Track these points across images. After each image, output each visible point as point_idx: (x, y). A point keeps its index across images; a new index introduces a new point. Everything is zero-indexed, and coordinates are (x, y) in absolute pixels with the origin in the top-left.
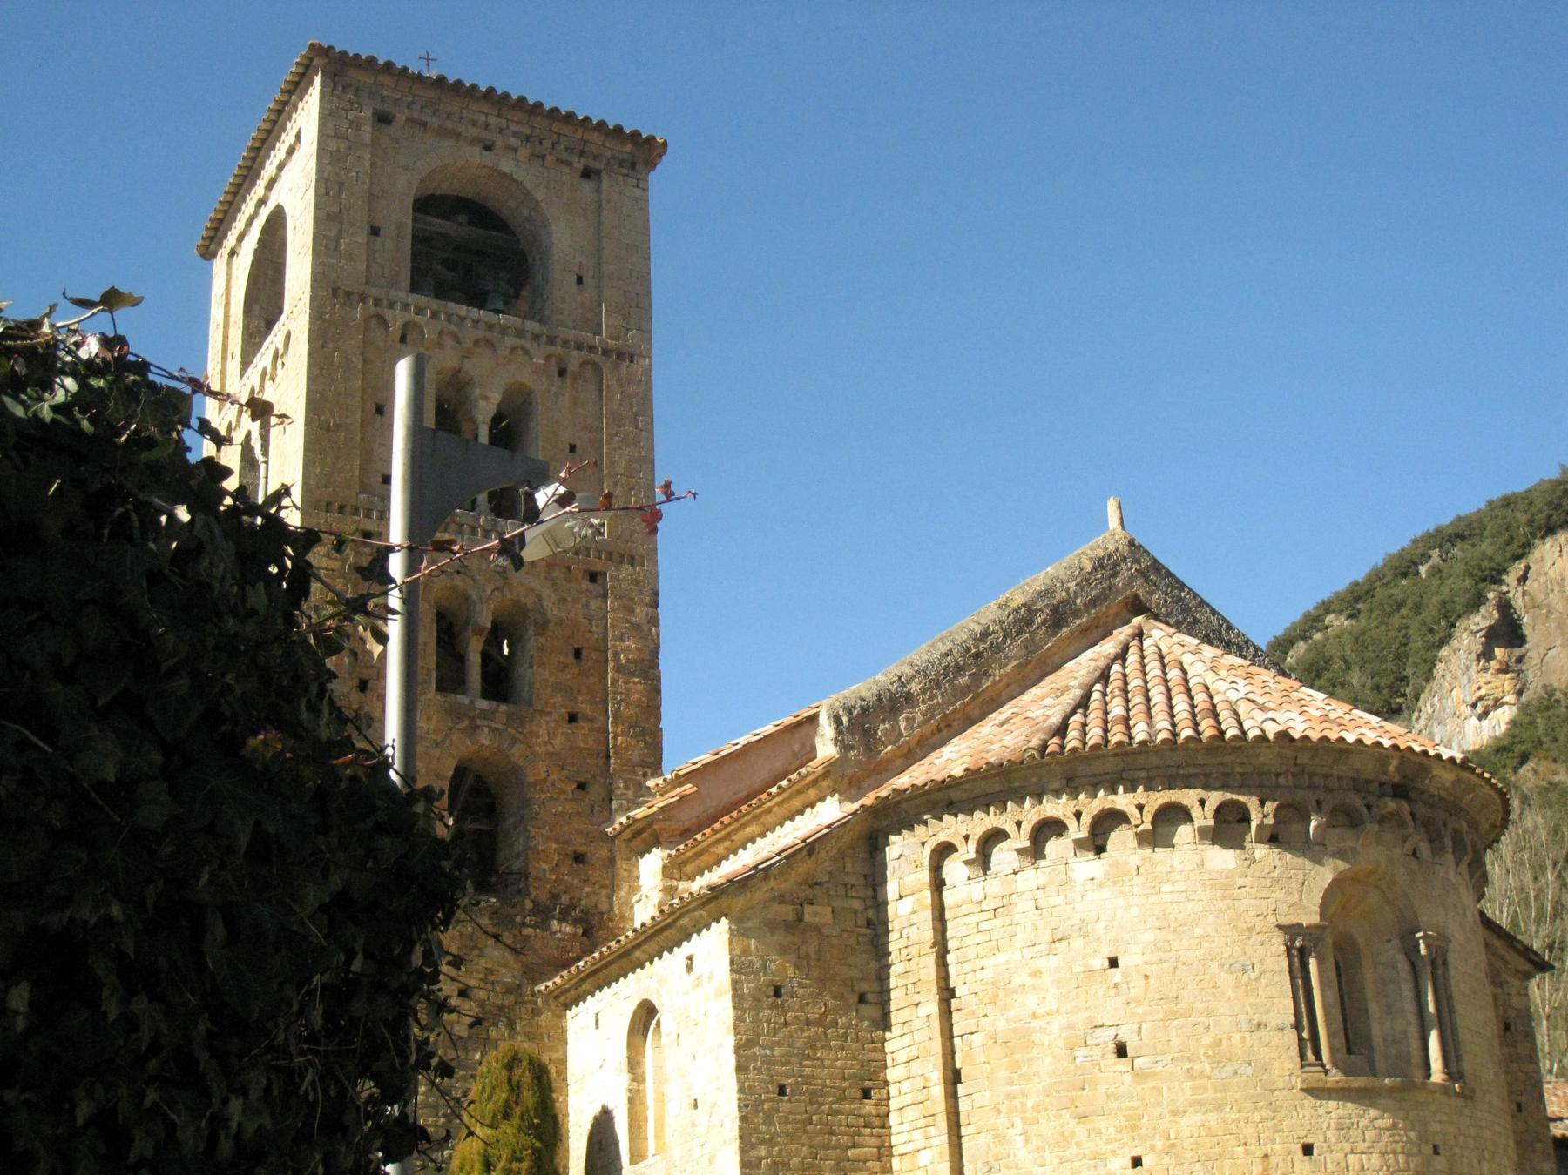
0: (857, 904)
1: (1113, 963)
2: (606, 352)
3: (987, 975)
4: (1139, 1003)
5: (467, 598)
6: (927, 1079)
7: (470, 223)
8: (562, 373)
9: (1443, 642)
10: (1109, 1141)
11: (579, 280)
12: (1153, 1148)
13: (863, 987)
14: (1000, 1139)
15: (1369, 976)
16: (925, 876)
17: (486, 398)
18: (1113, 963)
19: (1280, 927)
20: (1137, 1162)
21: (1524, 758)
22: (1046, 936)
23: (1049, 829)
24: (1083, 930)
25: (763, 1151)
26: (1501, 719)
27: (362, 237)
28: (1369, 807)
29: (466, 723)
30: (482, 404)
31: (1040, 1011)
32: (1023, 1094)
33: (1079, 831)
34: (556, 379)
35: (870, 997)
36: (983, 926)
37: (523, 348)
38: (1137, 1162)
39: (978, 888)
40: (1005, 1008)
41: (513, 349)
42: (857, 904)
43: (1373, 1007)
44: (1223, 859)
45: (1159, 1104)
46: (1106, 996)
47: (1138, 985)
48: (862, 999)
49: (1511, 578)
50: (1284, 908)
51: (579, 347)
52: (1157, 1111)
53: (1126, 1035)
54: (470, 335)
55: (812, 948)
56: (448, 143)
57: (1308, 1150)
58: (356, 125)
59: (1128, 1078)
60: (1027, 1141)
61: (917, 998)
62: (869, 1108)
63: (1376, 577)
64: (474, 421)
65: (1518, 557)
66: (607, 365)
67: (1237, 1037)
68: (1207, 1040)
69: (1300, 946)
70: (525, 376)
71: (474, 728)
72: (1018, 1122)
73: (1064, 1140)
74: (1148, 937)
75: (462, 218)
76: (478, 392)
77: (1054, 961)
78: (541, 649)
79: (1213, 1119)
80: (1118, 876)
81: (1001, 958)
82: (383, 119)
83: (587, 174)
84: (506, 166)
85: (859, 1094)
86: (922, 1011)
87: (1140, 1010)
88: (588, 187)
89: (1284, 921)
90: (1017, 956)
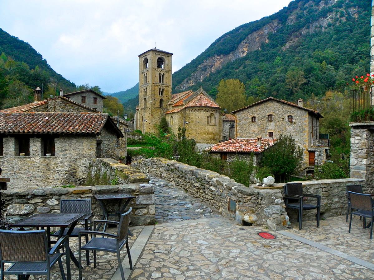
9: (240, 43)
21: (247, 59)
26: (246, 54)
44: (205, 112)
49: (249, 36)
54: (161, 70)
63: (233, 30)
65: (251, 33)
69: (208, 117)
70: (164, 73)
82: (155, 54)
83: (168, 57)
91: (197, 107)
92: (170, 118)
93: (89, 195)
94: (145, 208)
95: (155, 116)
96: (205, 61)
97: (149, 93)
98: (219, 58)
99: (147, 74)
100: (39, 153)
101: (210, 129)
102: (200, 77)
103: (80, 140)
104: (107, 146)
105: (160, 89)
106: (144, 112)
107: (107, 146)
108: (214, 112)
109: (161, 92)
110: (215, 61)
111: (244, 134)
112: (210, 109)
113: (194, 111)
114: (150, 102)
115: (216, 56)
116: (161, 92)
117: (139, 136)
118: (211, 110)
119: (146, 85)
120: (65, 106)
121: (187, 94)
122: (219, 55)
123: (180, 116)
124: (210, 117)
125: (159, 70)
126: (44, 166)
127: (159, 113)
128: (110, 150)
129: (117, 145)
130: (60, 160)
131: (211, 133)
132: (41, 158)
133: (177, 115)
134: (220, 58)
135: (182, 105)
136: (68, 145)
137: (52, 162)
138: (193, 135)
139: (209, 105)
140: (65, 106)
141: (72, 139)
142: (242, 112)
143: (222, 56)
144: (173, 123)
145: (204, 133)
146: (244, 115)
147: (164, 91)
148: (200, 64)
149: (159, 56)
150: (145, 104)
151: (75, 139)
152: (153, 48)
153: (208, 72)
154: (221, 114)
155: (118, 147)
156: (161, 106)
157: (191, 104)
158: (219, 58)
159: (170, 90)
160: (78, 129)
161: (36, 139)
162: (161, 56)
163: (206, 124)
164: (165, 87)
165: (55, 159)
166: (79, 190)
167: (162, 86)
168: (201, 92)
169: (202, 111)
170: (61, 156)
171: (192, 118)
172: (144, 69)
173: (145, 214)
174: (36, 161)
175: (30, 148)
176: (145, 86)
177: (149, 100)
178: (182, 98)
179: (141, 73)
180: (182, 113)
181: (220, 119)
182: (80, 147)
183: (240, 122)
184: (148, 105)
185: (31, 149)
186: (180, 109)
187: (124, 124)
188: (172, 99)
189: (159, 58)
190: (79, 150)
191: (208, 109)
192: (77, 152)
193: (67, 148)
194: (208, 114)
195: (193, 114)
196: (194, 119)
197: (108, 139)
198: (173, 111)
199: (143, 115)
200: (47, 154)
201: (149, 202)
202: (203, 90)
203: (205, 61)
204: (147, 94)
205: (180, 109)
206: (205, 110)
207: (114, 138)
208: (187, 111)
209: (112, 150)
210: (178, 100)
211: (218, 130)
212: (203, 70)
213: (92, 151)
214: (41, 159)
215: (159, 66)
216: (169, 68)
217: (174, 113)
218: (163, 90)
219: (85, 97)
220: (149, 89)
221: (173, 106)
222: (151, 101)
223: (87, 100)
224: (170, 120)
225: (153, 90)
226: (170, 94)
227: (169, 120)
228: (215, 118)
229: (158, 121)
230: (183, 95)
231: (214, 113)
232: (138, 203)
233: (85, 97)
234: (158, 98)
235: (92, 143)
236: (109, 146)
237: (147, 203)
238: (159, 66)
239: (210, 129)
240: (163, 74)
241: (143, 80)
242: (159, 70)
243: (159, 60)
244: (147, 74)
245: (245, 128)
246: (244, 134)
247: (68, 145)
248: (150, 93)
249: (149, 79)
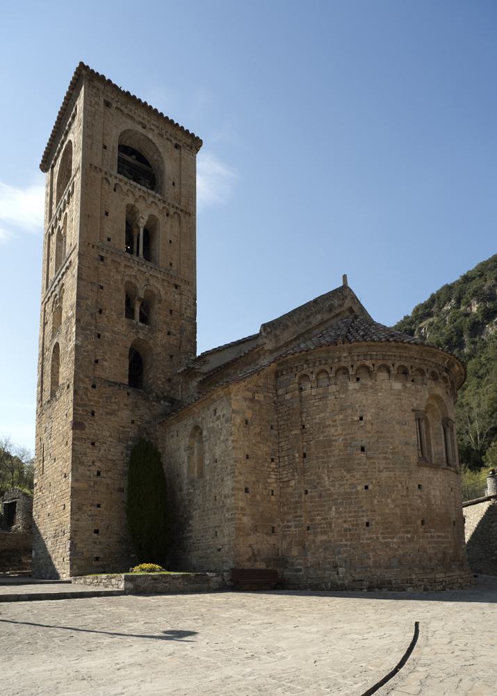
0: (271, 395)
1: (361, 419)
2: (181, 210)
3: (316, 421)
4: (369, 432)
5: (136, 287)
6: (295, 456)
7: (137, 159)
8: (168, 215)
10: (357, 479)
11: (174, 184)
12: (372, 483)
13: (273, 424)
14: (319, 477)
16: (297, 386)
17: (143, 218)
18: (361, 419)
19: (413, 410)
20: (366, 487)
22: (338, 408)
24: (351, 407)
25: (241, 478)
28: (440, 374)
29: (135, 330)
30: (141, 220)
31: (336, 434)
32: (328, 462)
34: (166, 217)
35: (274, 427)
36: (317, 404)
37: (155, 203)
38: (366, 487)
39: (314, 392)
40: (323, 432)
41: (152, 202)
42: (271, 395)
44: (397, 386)
45: (375, 468)
46: (358, 429)
47: (369, 427)
48: (272, 428)
50: (415, 405)
51: (173, 207)
52: (374, 470)
53: (363, 443)
55: (257, 407)
57: (420, 486)
59: (365, 459)
60: (329, 478)
61: (291, 428)
62: (273, 465)
64: (138, 227)
66: (182, 215)
67: (400, 447)
68: (391, 447)
69: (420, 418)
70: (156, 213)
71: (137, 332)
72: (326, 472)
73: (342, 478)
74: (373, 410)
75: (134, 157)
76: (140, 215)
77: (341, 417)
78: (159, 308)
79: (393, 473)
81: (322, 415)
83: (177, 146)
85: (270, 460)
86: (293, 433)
87: (370, 435)
88: (177, 151)
89: (414, 408)
90: (328, 414)
92: (185, 442)
123: (249, 415)
163: (414, 458)
195: (324, 398)
196: (336, 433)
216: (184, 200)
224: (184, 456)
227: (184, 456)
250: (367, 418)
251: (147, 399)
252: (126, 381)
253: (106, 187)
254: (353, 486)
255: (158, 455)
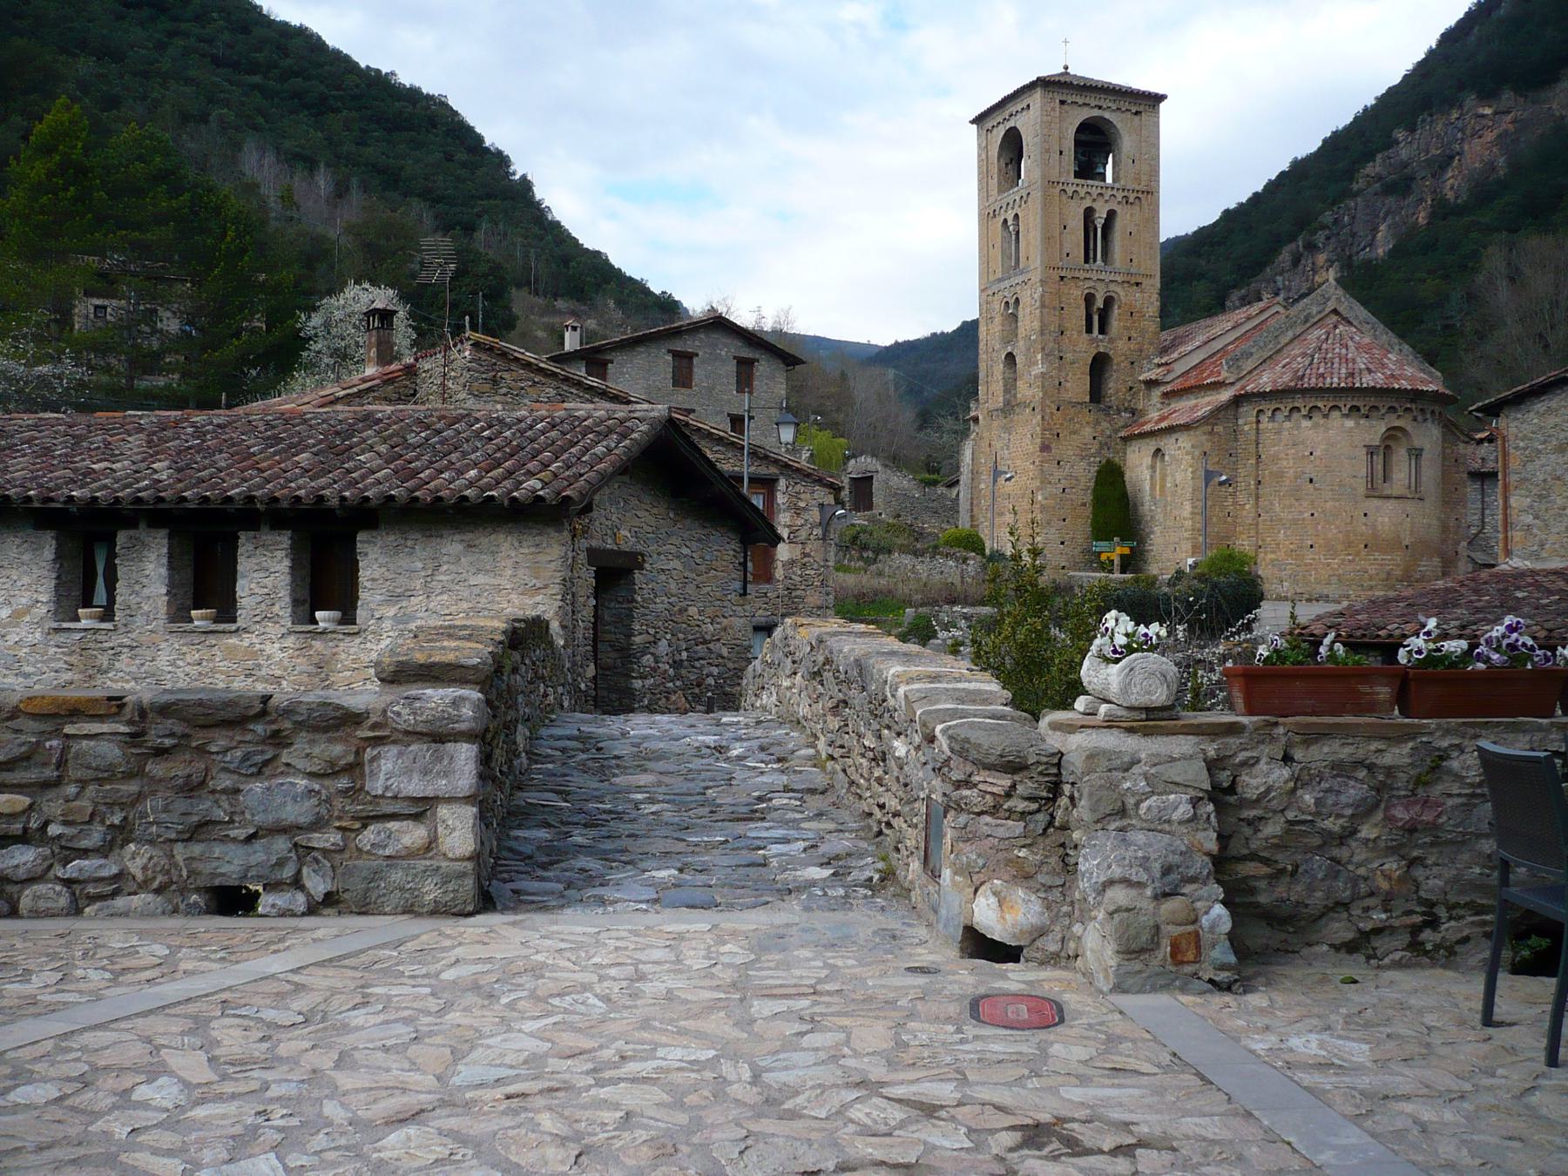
15: (1394, 458)
23: (1295, 409)
27: (1057, 156)
33: (1304, 412)
39: (1270, 425)
43: (1395, 469)
44: (1350, 423)
54: (1095, 192)
56: (1086, 109)
58: (1053, 109)
69: (1371, 451)
80: (1316, 426)
82: (1062, 102)
83: (1137, 113)
84: (1107, 115)
88: (1137, 118)
91: (1304, 392)
92: (1148, 460)
93: (105, 728)
94: (417, 817)
95: (1067, 449)
96: (1400, 135)
97: (1029, 321)
98: (1488, 111)
99: (1016, 216)
100: (283, 608)
101: (1386, 517)
102: (1375, 230)
103: (484, 540)
104: (673, 586)
105: (1089, 299)
106: (1008, 430)
107: (673, 586)
108: (1409, 417)
109: (1099, 316)
110: (1462, 130)
111: (1552, 538)
112: (1383, 405)
113: (1288, 418)
114: (1034, 368)
115: (1470, 100)
116: (1099, 316)
117: (965, 560)
118: (1392, 409)
119: (1014, 281)
120: (495, 381)
121: (1249, 319)
122: (1487, 95)
123: (1207, 446)
124: (1383, 451)
125: (1082, 192)
126: (304, 678)
127: (1088, 432)
128: (693, 611)
129: (737, 585)
130: (383, 645)
131: (1393, 545)
132: (290, 633)
133: (1185, 441)
134: (1496, 113)
135: (1218, 386)
136: (419, 565)
137: (343, 656)
138: (1281, 555)
139: (1377, 379)
140: (495, 381)
141: (442, 537)
142: (1540, 406)
143: (1507, 97)
144: (1163, 487)
145: (1349, 544)
146: (1552, 420)
147: (1116, 311)
148: (1369, 156)
149: (1086, 114)
150: (1010, 386)
151: (457, 537)
152: (1052, 69)
153: (1421, 200)
154: (1451, 430)
155: (745, 594)
156: (1096, 394)
157: (1266, 381)
158: (1488, 111)
159: (1148, 300)
160: (471, 484)
161: (268, 537)
162: (1096, 113)
163: (1362, 490)
164: (1118, 289)
165: (358, 640)
166: (55, 699)
167: (1100, 281)
168: (1331, 306)
169: (1336, 414)
170: (387, 624)
171: (1275, 458)
172: (1000, 191)
173: (410, 854)
174: (269, 648)
175: (240, 583)
176: (1007, 284)
177: (1031, 363)
178: (1217, 345)
179: (987, 216)
180: (1219, 429)
181: (1450, 463)
182: (481, 579)
183: (1530, 467)
184: (1027, 390)
185: (243, 588)
186: (1204, 404)
187: (820, 481)
188: (1164, 351)
189: (1084, 127)
190: (476, 591)
191: (1373, 401)
192: (465, 605)
193: (418, 584)
194: (1375, 431)
195: (1278, 433)
196: (1288, 465)
197: (685, 551)
198: (1162, 419)
199: (998, 445)
200: (319, 614)
201: (441, 786)
202: (1340, 292)
203: (1400, 135)
204: (1021, 332)
205: (1204, 404)
206: (1355, 409)
207: (723, 550)
208: (1248, 413)
209: (710, 611)
210: (1195, 359)
211: (1435, 522)
212: (1390, 189)
213: (539, 598)
214: (290, 641)
215: (1087, 168)
216: (1144, 178)
217: (1171, 430)
218: (1109, 301)
219: (690, 357)
220: (1030, 298)
221: (1166, 395)
222: (1039, 368)
223: (699, 372)
224: (1147, 474)
225: (1052, 305)
226: (1152, 326)
228: (1416, 453)
229: (1084, 474)
230: (1229, 325)
231: (1409, 428)
232: (376, 786)
233: (690, 357)
234: (1083, 348)
235: (541, 558)
236: (690, 589)
237: (429, 793)
238: (1087, 168)
239: (1386, 517)
240: (1111, 215)
241: (997, 254)
242: (1082, 192)
243: (1083, 137)
244: (1016, 216)
245: (1560, 501)
246: (1552, 538)
247: (419, 565)
248: (1036, 325)
249: (1028, 244)
250: (1317, 453)
251: (1108, 415)
252: (1087, 399)
253: (1064, 197)
254: (1301, 513)
255: (1122, 475)
